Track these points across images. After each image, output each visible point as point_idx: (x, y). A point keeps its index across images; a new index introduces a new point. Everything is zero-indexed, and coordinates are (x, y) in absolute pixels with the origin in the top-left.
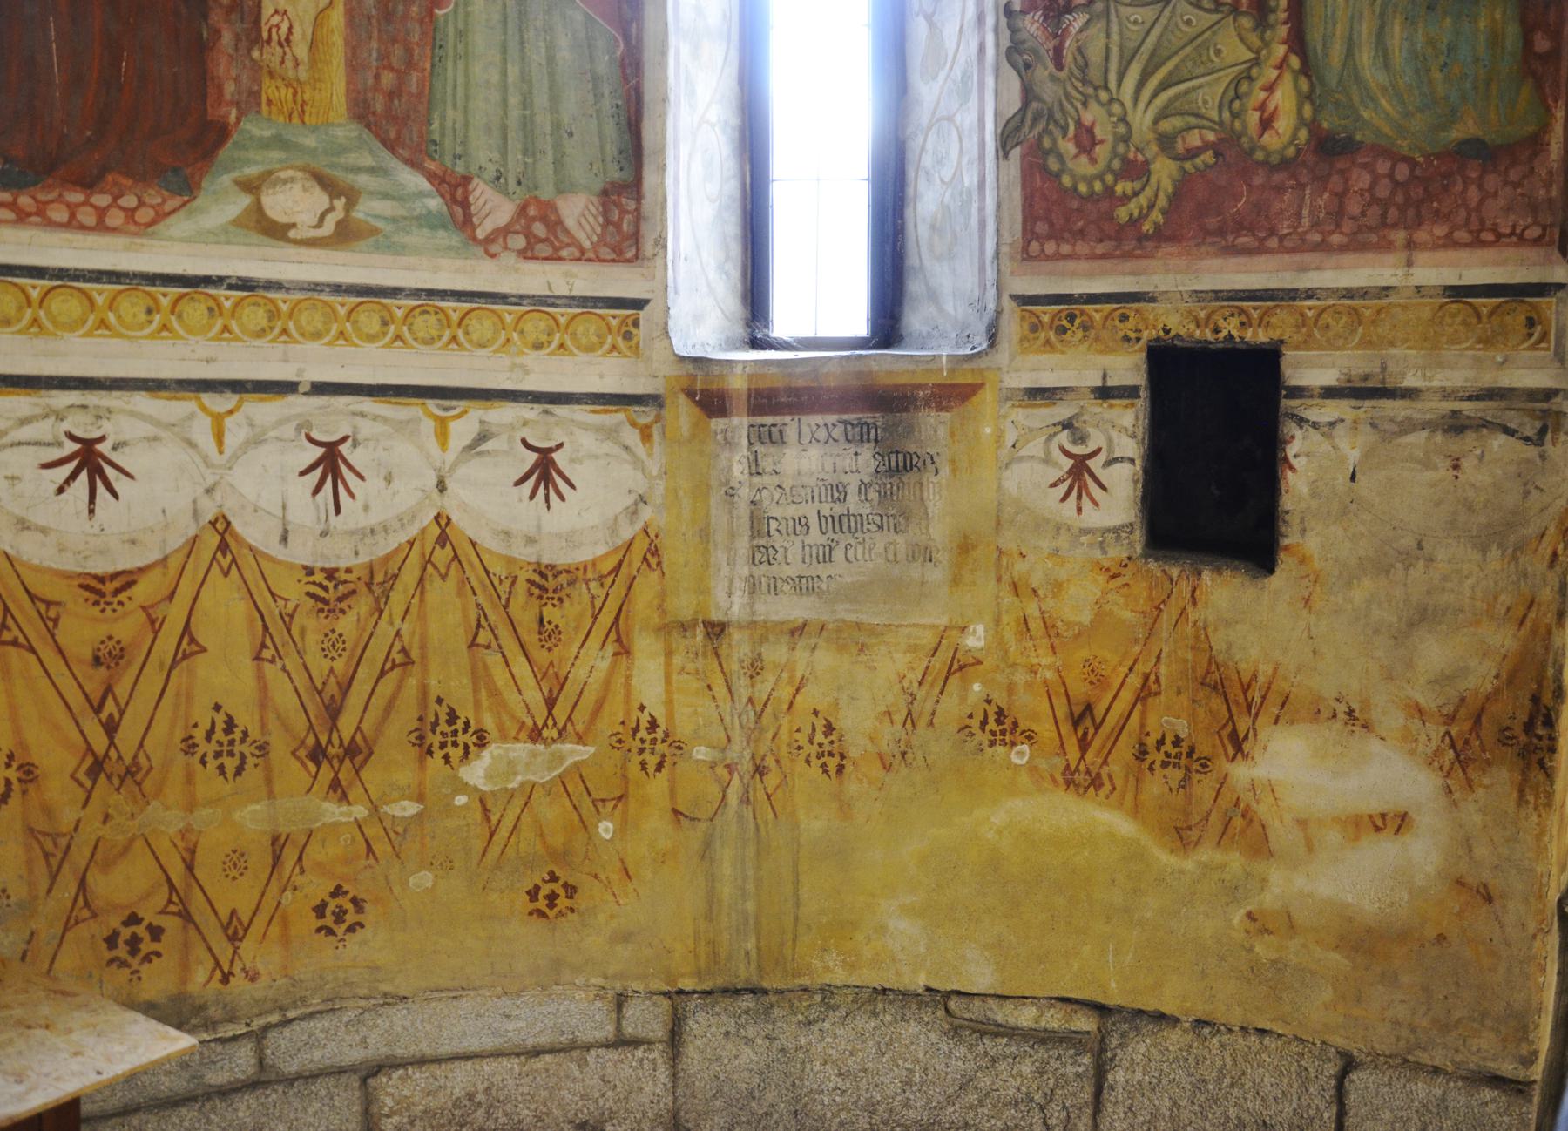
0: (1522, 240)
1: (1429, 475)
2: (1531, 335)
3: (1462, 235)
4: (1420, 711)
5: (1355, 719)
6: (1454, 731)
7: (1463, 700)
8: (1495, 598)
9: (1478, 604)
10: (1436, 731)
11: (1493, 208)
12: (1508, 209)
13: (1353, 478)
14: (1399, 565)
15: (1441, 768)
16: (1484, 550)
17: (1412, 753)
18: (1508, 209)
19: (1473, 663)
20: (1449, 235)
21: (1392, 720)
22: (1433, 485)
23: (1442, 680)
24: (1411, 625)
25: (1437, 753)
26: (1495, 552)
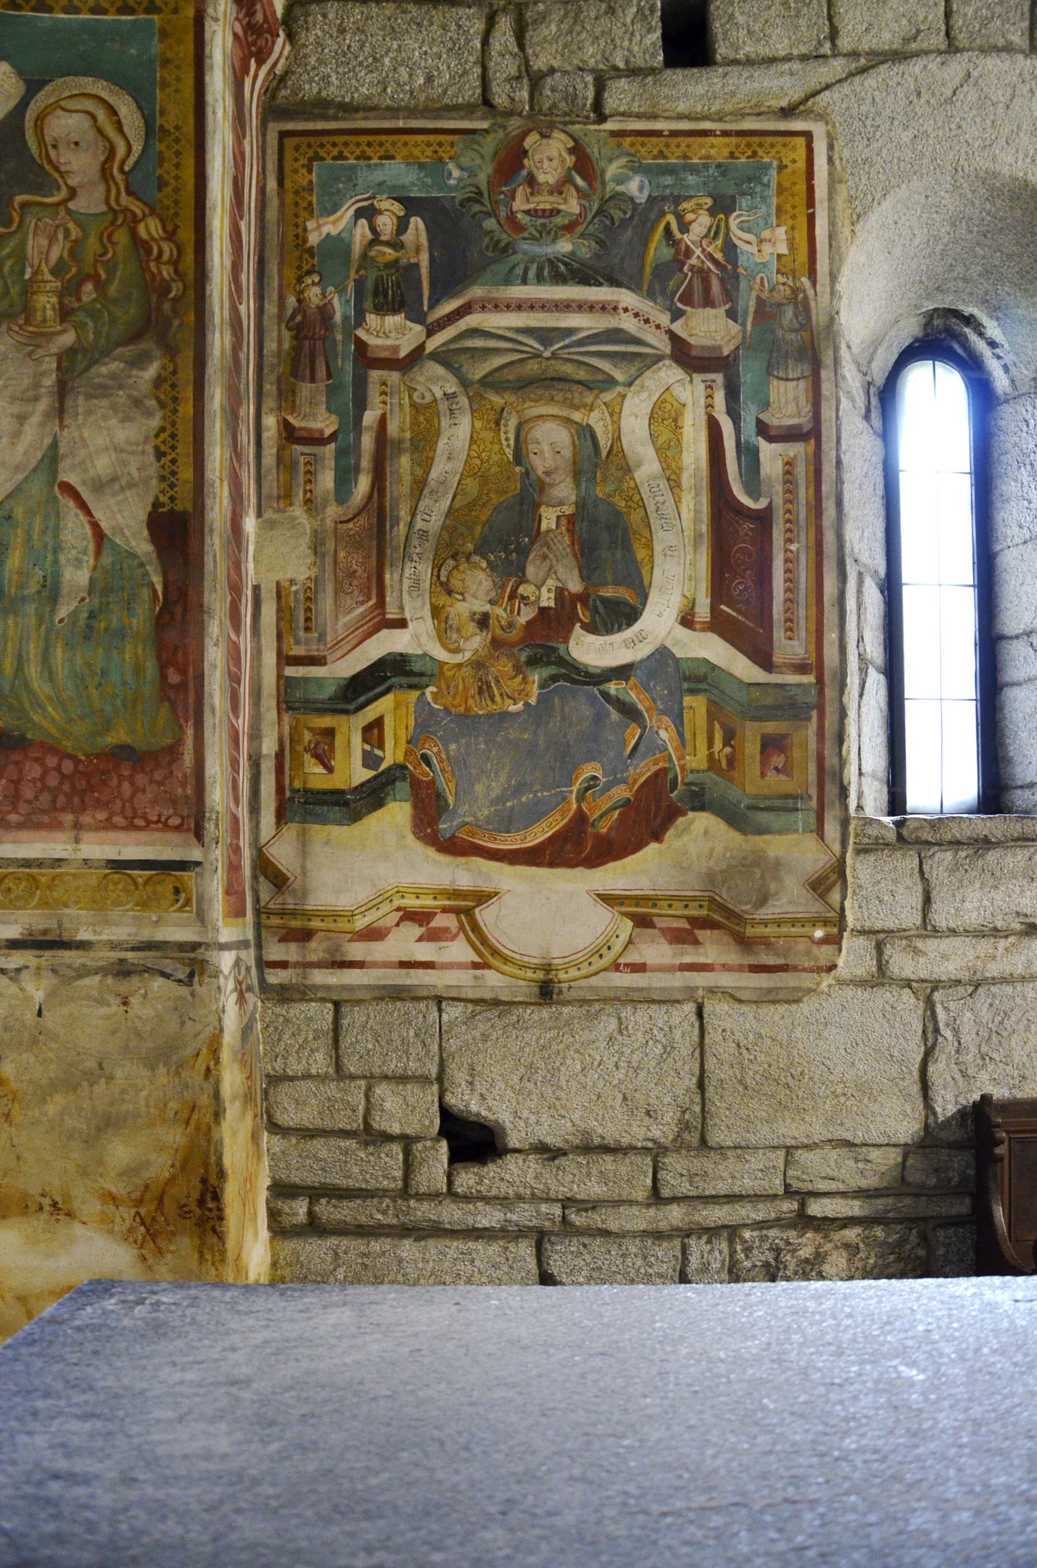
0: (166, 827)
1: (104, 1011)
2: (178, 901)
3: (118, 820)
4: (114, 1199)
5: (59, 1209)
6: (143, 1211)
7: (147, 1186)
8: (165, 1105)
9: (152, 1110)
10: (127, 1213)
11: (142, 801)
12: (153, 803)
13: (40, 1014)
14: (85, 1083)
15: (135, 1242)
16: (153, 1068)
17: (111, 1232)
18: (153, 803)
19: (153, 1157)
20: (108, 819)
21: (92, 1207)
22: (107, 1018)
23: (128, 1172)
24: (99, 1129)
25: (131, 1230)
26: (162, 1070)
